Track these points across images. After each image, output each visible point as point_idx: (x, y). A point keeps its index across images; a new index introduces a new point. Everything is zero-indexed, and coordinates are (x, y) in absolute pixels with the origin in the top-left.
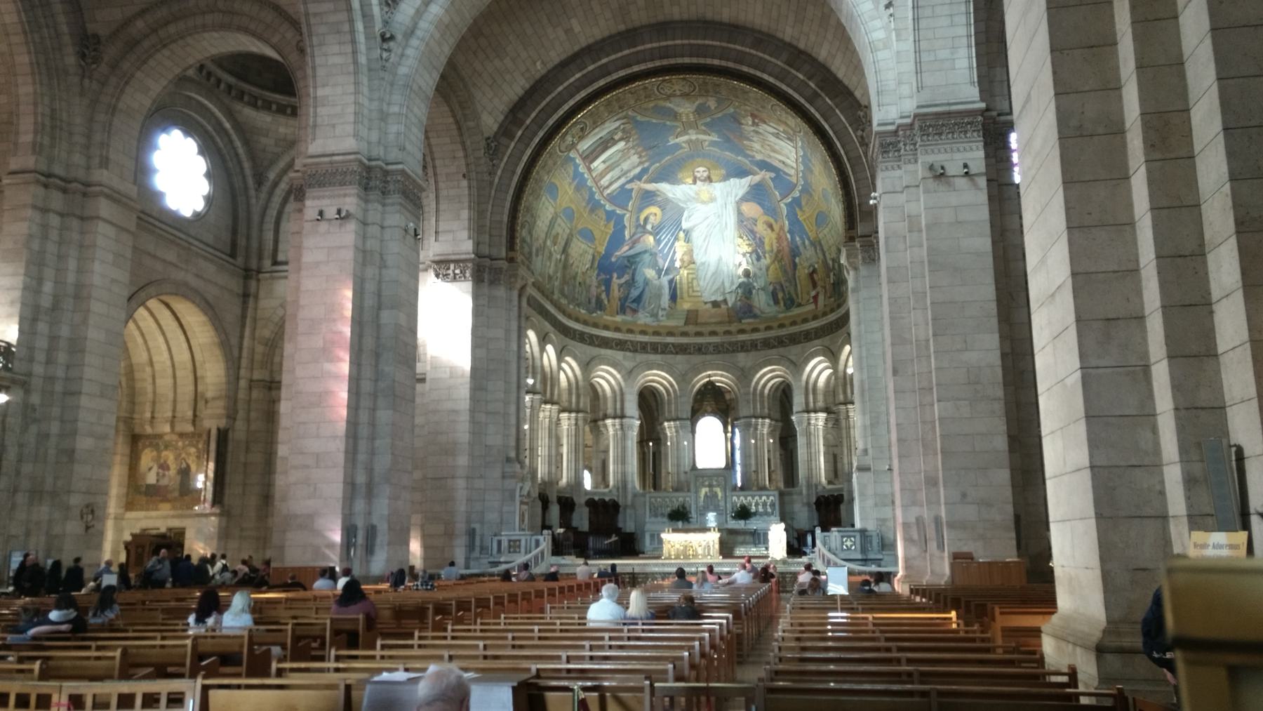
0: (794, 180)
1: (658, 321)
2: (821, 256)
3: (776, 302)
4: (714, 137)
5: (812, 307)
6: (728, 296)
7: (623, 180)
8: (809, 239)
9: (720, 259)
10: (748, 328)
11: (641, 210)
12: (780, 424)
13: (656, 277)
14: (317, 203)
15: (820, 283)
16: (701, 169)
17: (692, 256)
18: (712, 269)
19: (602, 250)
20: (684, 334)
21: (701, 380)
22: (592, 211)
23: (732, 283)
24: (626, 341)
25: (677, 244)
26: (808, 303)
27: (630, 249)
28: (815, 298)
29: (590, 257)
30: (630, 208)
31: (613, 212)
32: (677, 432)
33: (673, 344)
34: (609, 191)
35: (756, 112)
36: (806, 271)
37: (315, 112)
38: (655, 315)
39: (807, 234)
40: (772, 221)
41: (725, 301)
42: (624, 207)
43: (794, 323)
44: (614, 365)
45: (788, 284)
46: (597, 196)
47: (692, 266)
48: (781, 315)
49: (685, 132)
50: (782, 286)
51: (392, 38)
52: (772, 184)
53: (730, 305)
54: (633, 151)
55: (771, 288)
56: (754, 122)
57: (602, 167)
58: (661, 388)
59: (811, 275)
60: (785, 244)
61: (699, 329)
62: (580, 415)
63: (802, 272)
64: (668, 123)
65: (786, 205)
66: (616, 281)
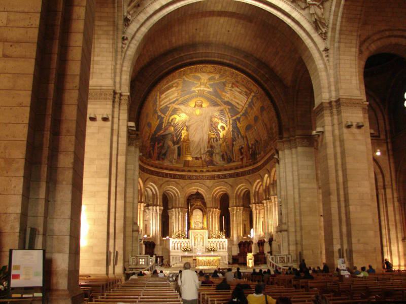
0: (240, 111)
1: (173, 164)
2: (246, 142)
3: (224, 159)
4: (211, 90)
5: (240, 163)
6: (202, 156)
7: (168, 103)
8: (241, 135)
9: (200, 139)
10: (210, 170)
11: (171, 116)
12: (220, 211)
13: (173, 145)
14: (92, 106)
15: (244, 153)
16: (199, 102)
17: (188, 137)
18: (196, 144)
19: (153, 132)
20: (183, 171)
21: (193, 189)
22: (153, 115)
23: (205, 150)
24: (160, 172)
25: (183, 131)
26: (238, 161)
27: (164, 132)
28: (242, 159)
29: (148, 134)
30: (167, 115)
31: (160, 116)
32: (179, 213)
33: (178, 175)
34: (161, 107)
35: (235, 83)
36: (238, 148)
37: (93, 67)
38: (171, 162)
39: (240, 133)
40: (225, 126)
41: (201, 158)
42: (164, 114)
43: (231, 169)
44: (154, 183)
45: (229, 152)
46: (157, 109)
47: (188, 141)
48: (225, 165)
49: (200, 86)
50: (226, 153)
51: (127, 39)
52: (228, 110)
53: (203, 159)
54: (176, 92)
55: (221, 154)
56: (232, 87)
57: (164, 97)
58: (172, 194)
59: (240, 150)
60: (229, 135)
61: (189, 169)
62: (143, 204)
63: (236, 148)
64: (195, 82)
65: (233, 120)
66: (157, 146)
